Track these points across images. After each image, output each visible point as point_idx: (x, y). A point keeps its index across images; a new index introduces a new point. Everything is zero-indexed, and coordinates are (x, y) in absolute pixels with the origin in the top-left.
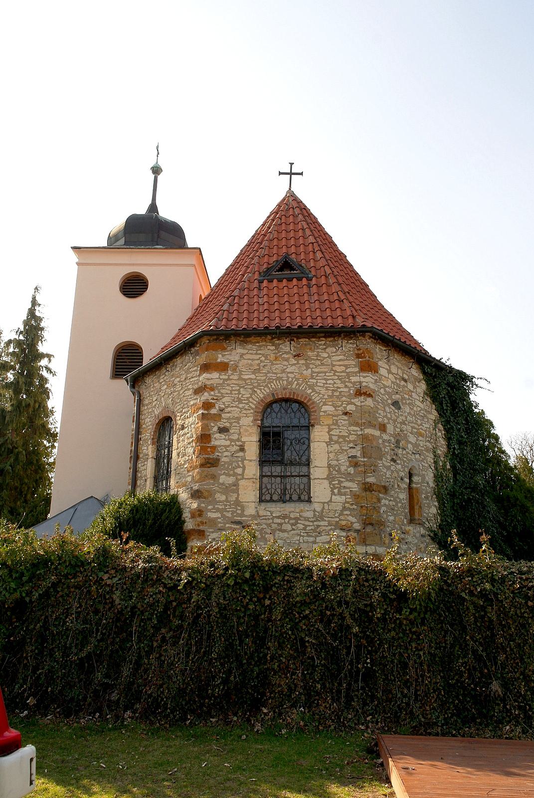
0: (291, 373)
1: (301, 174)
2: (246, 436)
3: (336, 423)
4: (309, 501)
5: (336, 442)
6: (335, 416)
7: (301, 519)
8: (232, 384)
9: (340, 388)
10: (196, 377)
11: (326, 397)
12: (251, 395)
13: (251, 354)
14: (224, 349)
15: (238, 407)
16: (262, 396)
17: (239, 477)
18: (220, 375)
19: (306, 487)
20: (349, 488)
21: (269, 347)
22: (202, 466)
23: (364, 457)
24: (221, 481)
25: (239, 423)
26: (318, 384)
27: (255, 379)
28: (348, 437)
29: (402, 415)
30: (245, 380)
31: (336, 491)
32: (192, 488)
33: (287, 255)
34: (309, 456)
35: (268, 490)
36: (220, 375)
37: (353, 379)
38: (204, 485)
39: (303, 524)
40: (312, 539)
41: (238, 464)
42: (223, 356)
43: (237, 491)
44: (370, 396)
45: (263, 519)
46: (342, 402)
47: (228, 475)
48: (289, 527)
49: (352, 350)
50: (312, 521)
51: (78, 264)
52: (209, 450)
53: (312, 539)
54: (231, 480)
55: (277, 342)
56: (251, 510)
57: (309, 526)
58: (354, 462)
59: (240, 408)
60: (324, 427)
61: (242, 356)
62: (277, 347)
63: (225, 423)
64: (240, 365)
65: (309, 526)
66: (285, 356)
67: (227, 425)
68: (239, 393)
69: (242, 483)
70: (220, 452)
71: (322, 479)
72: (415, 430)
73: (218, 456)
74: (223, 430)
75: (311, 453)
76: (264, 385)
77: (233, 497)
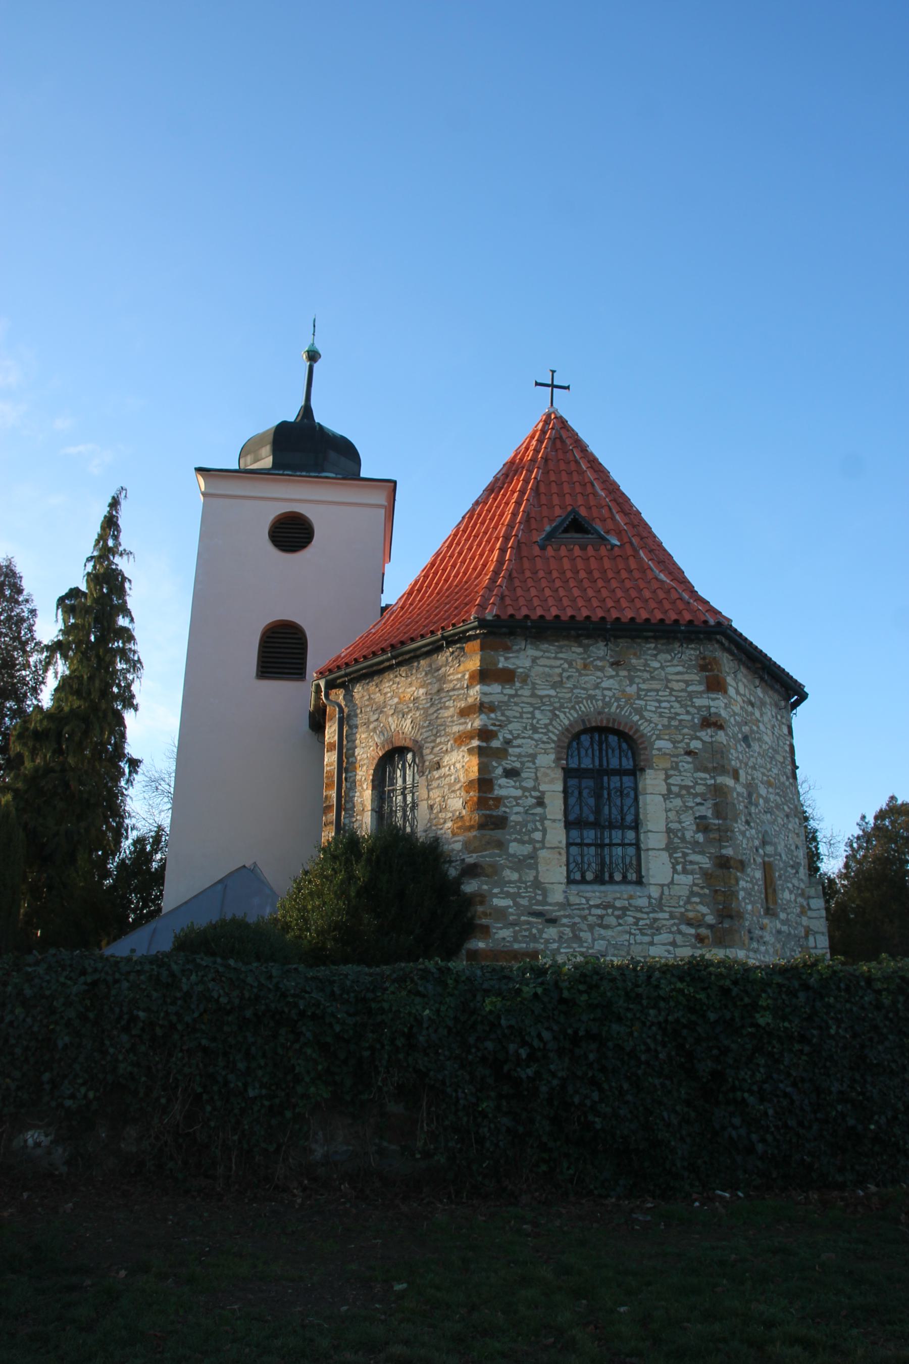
0: (610, 689)
1: (568, 388)
2: (545, 783)
3: (676, 767)
4: (639, 882)
5: (678, 795)
6: (674, 756)
7: (631, 909)
8: (523, 702)
9: (679, 714)
10: (462, 688)
11: (660, 727)
12: (551, 720)
13: (548, 658)
14: (508, 649)
15: (532, 739)
16: (567, 722)
17: (538, 845)
18: (503, 688)
19: (634, 862)
20: (697, 863)
21: (574, 649)
22: (481, 826)
23: (718, 818)
24: (511, 851)
25: (534, 763)
26: (648, 708)
27: (556, 696)
28: (693, 787)
29: (752, 756)
30: (541, 697)
31: (679, 868)
32: (464, 860)
33: (574, 511)
34: (637, 815)
35: (577, 864)
36: (503, 688)
37: (698, 702)
38: (482, 857)
39: (634, 917)
40: (647, 939)
41: (536, 826)
42: (507, 659)
43: (535, 867)
44: (721, 727)
46: (684, 735)
47: (523, 842)
48: (612, 921)
49: (693, 658)
50: (647, 913)
51: (204, 494)
52: (491, 802)
53: (647, 939)
54: (527, 849)
55: (586, 641)
56: (557, 895)
57: (643, 919)
58: (702, 825)
59: (536, 741)
60: (659, 772)
61: (534, 660)
62: (586, 648)
63: (514, 762)
64: (533, 674)
65: (643, 919)
66: (599, 663)
67: (517, 765)
68: (533, 717)
69: (542, 854)
70: (506, 807)
71: (659, 850)
72: (765, 778)
73: (505, 812)
74: (511, 773)
75: (641, 810)
76: (570, 705)
77: (530, 876)
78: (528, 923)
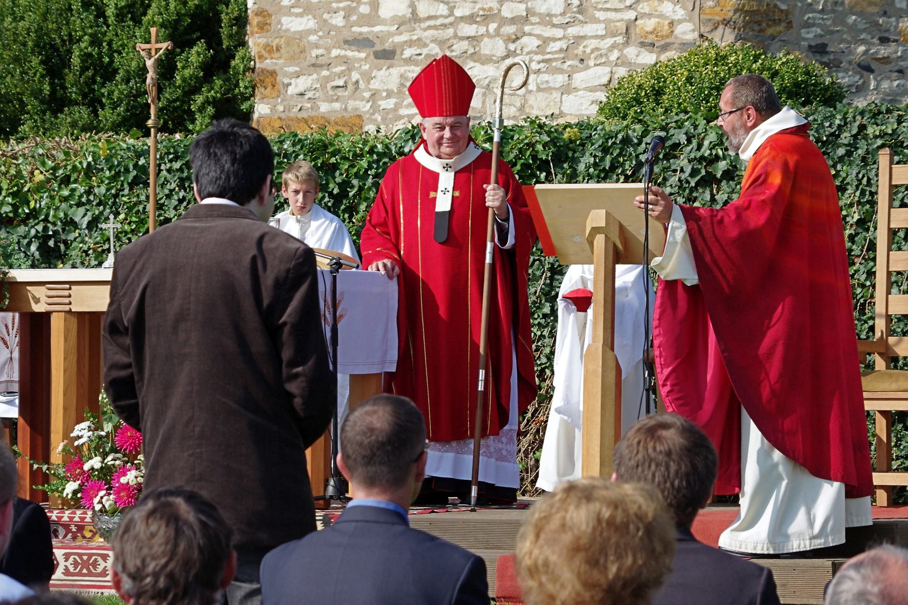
39: (538, 37)
40: (561, 79)
45: (430, 27)
53: (561, 79)
57: (555, 40)
65: (555, 40)
78: (346, 61)
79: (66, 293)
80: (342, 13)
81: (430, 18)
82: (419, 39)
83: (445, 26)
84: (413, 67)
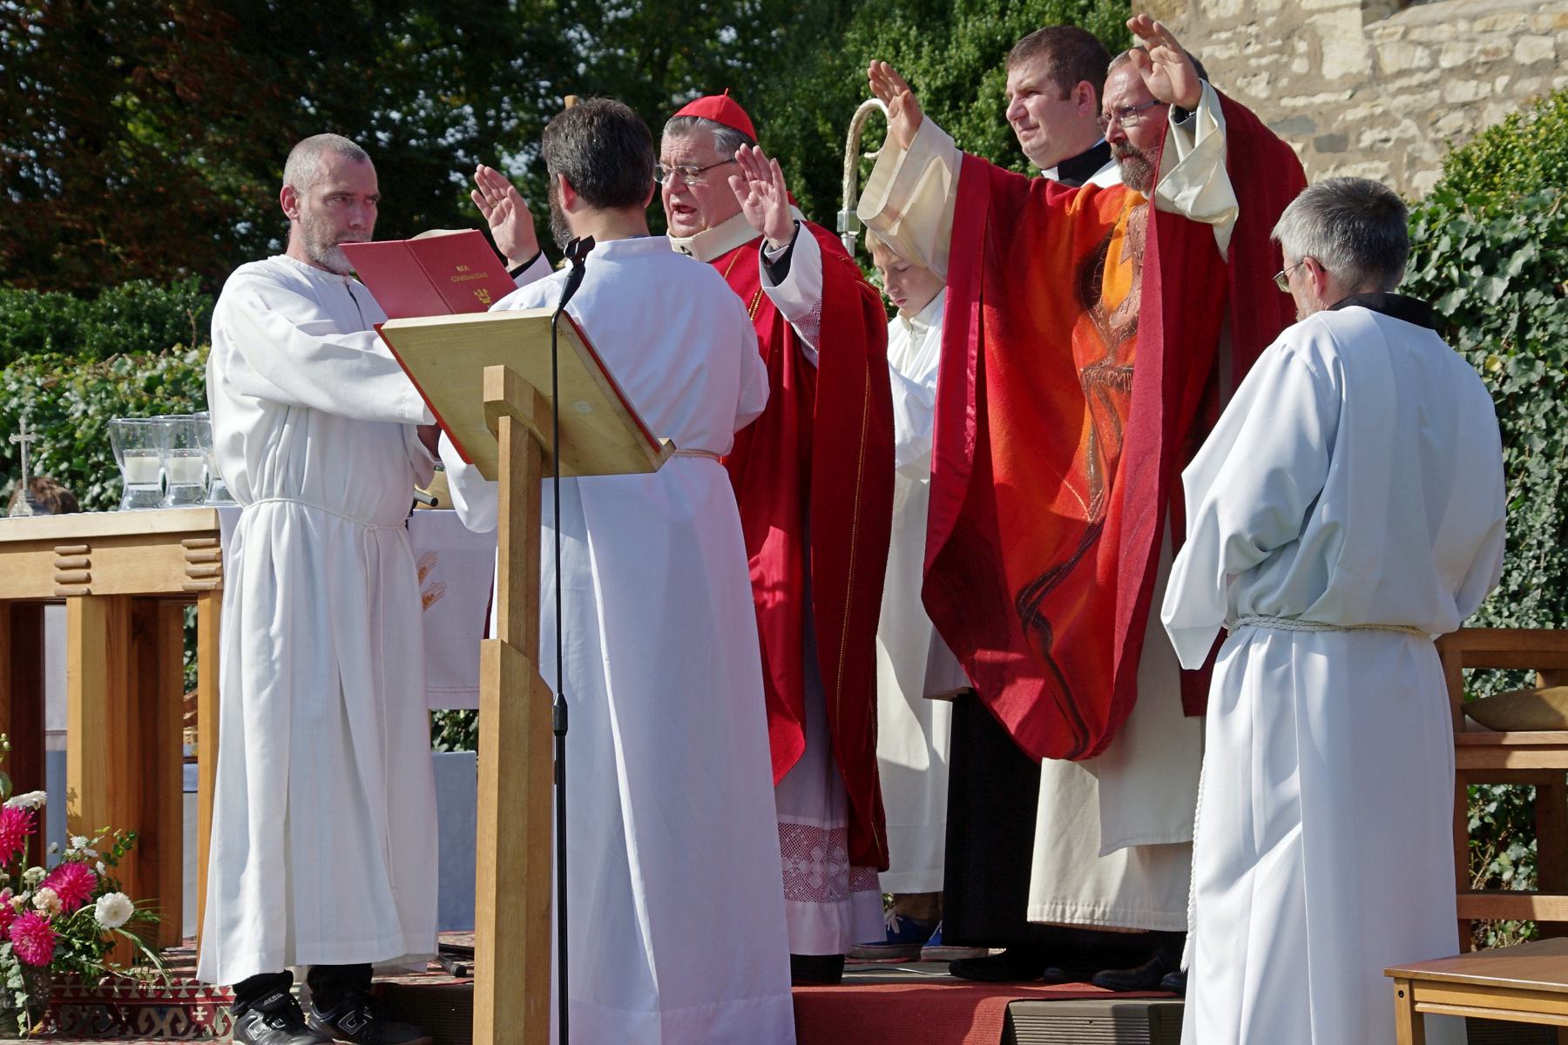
45: (1401, 91)
79: (83, 559)
80: (1265, 76)
81: (1401, 73)
82: (1385, 113)
83: (1425, 86)
84: (1377, 164)
